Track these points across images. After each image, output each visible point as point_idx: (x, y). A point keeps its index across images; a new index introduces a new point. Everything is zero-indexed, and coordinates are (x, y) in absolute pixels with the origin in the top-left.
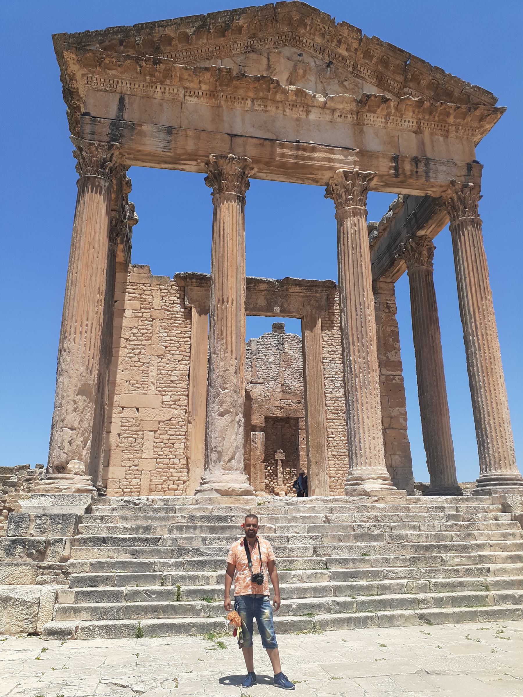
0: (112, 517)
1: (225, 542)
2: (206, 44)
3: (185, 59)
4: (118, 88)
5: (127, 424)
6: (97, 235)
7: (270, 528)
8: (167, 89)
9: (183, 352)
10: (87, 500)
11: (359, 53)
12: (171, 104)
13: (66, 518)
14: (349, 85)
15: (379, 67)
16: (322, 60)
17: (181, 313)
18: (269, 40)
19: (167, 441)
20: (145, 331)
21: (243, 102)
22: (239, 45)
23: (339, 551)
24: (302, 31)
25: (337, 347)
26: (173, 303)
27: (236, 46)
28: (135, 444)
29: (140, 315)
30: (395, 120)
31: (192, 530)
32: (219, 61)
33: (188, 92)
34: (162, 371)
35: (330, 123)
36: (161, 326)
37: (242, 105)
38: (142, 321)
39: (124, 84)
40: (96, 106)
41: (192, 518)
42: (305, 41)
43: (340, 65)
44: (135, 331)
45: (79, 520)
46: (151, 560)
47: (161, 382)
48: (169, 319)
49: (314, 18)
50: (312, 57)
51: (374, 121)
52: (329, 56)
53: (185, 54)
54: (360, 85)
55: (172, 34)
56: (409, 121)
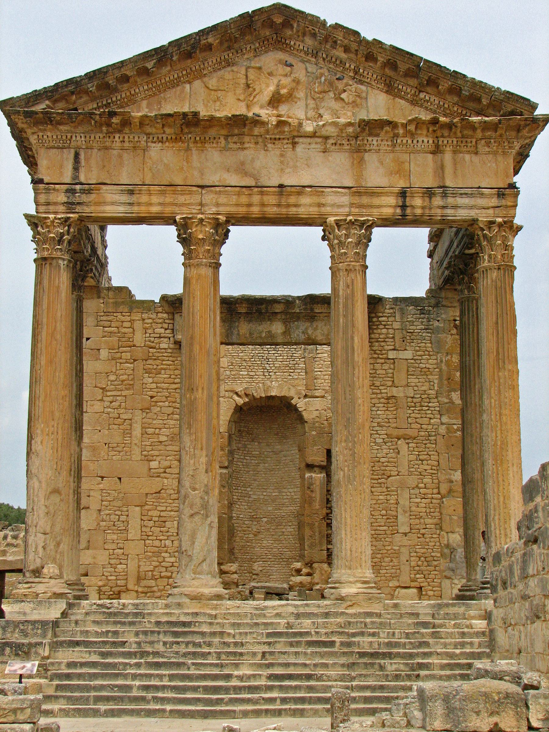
0: (84, 621)
1: (183, 646)
2: (169, 72)
3: (147, 92)
4: (72, 144)
5: (109, 499)
6: (58, 325)
7: (229, 634)
8: (126, 137)
9: (174, 402)
10: (62, 605)
11: (359, 56)
12: (132, 153)
13: (44, 623)
14: (348, 97)
15: (387, 70)
16: (316, 64)
17: (169, 351)
18: (248, 49)
19: (157, 519)
20: (125, 377)
21: (215, 141)
22: (210, 63)
23: (286, 656)
24: (289, 32)
25: (380, 388)
26: (160, 337)
27: (206, 65)
28: (119, 523)
29: (118, 355)
30: (404, 141)
31: (156, 635)
32: (188, 86)
33: (151, 138)
34: (148, 430)
35: (322, 154)
36: (144, 369)
37: (214, 145)
38: (121, 363)
39: (78, 138)
40: (49, 168)
41: (158, 623)
42: (292, 43)
43: (338, 69)
44: (112, 378)
45: (56, 624)
46: (116, 661)
47: (147, 443)
48: (155, 359)
49: (300, 20)
50: (303, 62)
51: (378, 146)
52: (324, 59)
53: (146, 87)
54: (364, 95)
55: (129, 73)
56: (423, 141)
